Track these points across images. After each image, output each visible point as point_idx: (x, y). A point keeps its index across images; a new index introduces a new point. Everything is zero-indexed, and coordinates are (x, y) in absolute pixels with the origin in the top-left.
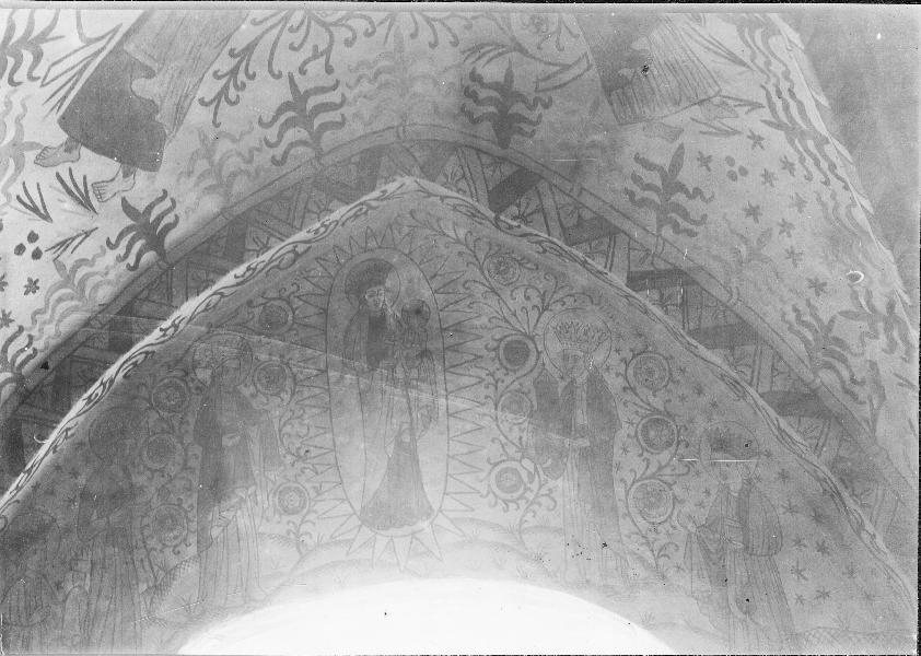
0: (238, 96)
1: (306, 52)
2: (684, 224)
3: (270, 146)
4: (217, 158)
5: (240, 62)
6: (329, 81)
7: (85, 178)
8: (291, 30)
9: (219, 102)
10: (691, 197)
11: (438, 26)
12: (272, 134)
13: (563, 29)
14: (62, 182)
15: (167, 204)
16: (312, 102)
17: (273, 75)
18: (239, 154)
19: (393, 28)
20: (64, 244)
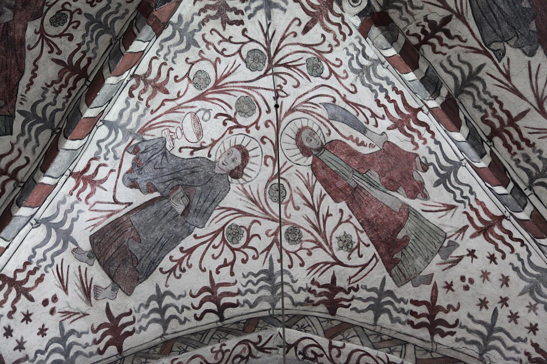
0: (180, 275)
1: (221, 261)
2: (446, 330)
3: (194, 308)
4: (163, 304)
5: (185, 256)
6: (231, 280)
7: (92, 278)
8: (214, 247)
9: (170, 274)
10: (446, 312)
11: (293, 256)
12: (196, 302)
13: (361, 243)
14: (80, 270)
15: (129, 319)
16: (220, 290)
17: (201, 268)
18: (176, 307)
19: (269, 256)
20: (67, 313)
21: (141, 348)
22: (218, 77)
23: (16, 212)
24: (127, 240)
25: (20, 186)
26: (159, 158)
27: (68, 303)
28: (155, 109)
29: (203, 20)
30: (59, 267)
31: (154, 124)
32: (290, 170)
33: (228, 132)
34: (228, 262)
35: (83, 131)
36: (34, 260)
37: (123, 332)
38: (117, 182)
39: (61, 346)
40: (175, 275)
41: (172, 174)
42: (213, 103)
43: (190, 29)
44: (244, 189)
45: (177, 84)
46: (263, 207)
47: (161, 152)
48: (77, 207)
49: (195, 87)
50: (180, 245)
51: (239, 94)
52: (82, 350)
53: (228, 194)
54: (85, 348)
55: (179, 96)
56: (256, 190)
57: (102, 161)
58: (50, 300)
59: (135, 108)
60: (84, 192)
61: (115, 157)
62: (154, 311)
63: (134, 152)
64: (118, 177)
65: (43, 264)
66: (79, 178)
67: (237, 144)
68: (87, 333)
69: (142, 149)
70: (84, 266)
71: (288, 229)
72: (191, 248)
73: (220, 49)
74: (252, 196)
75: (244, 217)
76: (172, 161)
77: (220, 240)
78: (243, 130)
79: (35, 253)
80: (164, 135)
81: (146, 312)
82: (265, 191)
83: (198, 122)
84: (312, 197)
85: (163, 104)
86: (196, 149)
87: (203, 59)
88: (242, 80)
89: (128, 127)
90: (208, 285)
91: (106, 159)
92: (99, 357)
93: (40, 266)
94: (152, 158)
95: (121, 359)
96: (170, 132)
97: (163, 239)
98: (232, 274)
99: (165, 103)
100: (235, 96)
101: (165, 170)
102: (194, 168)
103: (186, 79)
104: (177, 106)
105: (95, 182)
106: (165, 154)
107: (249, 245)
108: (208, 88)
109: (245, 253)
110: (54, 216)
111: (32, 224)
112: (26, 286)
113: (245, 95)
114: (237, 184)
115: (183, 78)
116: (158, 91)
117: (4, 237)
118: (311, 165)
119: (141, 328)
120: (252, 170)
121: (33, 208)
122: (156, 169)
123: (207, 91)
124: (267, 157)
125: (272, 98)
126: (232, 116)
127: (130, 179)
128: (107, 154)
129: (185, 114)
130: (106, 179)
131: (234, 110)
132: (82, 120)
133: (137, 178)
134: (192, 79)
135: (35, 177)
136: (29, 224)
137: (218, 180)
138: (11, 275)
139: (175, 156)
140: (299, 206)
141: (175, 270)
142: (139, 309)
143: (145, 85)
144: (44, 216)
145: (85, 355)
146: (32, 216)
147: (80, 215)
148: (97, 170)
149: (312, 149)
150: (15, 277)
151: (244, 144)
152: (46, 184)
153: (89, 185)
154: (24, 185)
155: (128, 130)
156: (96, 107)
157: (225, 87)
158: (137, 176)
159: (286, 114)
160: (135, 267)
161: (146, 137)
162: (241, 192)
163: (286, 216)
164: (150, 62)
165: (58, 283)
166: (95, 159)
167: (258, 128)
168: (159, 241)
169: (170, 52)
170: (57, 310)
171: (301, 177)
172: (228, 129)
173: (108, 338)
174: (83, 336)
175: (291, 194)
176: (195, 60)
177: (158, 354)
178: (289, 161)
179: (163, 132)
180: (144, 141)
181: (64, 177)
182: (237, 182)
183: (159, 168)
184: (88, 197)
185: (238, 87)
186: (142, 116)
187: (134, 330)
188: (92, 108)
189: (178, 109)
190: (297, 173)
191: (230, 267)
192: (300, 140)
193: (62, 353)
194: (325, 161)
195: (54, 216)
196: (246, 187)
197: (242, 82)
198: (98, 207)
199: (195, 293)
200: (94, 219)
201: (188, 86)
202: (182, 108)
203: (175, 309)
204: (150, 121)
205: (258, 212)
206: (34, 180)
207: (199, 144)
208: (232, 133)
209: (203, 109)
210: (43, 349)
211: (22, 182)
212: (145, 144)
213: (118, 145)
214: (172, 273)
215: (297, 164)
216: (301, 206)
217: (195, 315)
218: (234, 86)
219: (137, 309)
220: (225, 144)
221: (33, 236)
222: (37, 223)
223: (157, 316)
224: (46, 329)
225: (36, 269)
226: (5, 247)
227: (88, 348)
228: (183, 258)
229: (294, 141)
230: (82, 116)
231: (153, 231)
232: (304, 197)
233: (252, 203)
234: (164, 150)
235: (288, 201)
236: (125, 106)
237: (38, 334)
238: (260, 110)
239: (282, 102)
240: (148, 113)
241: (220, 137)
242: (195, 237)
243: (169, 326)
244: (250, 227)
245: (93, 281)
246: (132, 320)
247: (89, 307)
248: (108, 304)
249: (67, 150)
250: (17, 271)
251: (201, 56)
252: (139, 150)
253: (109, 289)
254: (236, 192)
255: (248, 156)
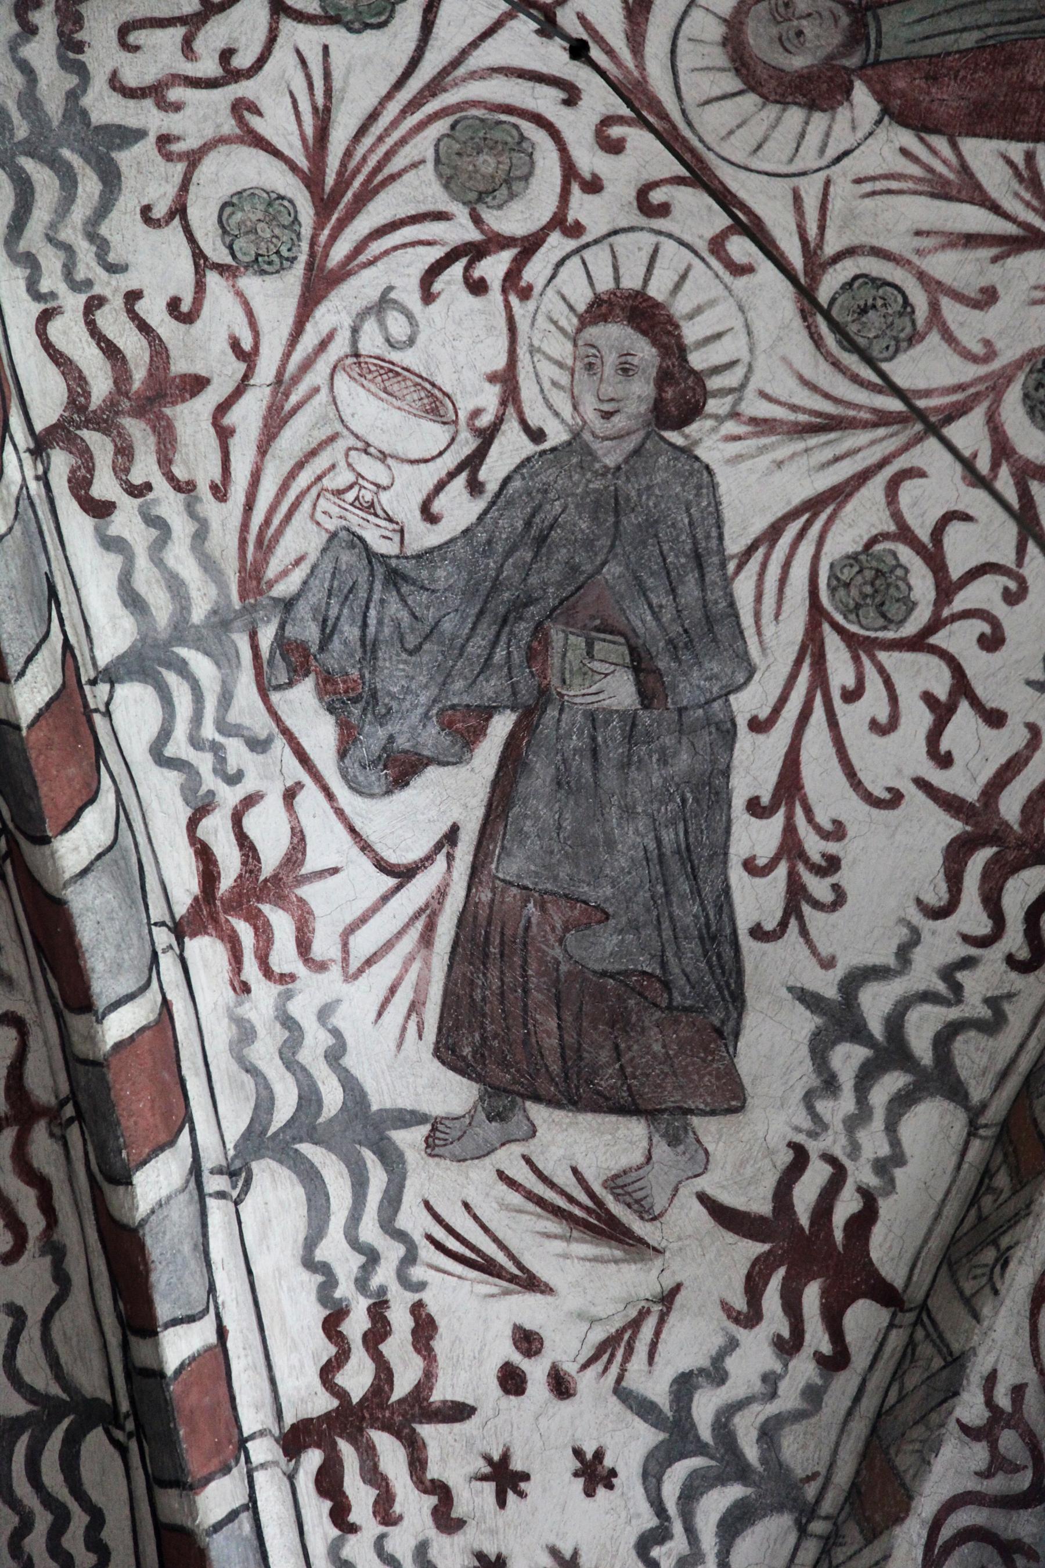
0: (836, 888)
4: (876, 1028)
5: (790, 818)
7: (575, 1171)
8: (851, 696)
9: (800, 918)
14: (512, 1183)
15: (816, 1175)
17: (877, 803)
18: (927, 997)
21: (945, 1227)
22: (303, 163)
23: (134, 1207)
24: (558, 952)
25: (71, 1121)
26: (394, 607)
27: (581, 1316)
28: (216, 475)
29: (60, 34)
30: (440, 1234)
31: (267, 522)
32: (836, 205)
33: (514, 300)
34: (942, 693)
35: (72, 771)
36: (345, 1289)
37: (839, 1235)
38: (340, 813)
39: (697, 1462)
40: (817, 905)
41: (481, 613)
42: (371, 263)
43: (54, 107)
44: (753, 421)
45: (199, 324)
46: (874, 411)
47: (378, 586)
48: (303, 1009)
49: (263, 272)
50: (739, 802)
51: (423, 145)
52: (772, 1409)
53: (722, 490)
54: (773, 1395)
55: (248, 357)
56: (792, 383)
57: (229, 797)
58: (517, 1358)
59: (154, 533)
60: (277, 945)
61: (258, 745)
62: (866, 1077)
63: (298, 670)
64: (330, 796)
65: (384, 1275)
66: (215, 920)
67: (581, 308)
68: (732, 1345)
69: (311, 633)
70: (509, 1158)
71: (1026, 396)
72: (782, 777)
73: (208, 67)
74: (802, 418)
75: (849, 507)
76: (441, 573)
77: (845, 655)
78: (557, 244)
79: (324, 1269)
80: (331, 525)
81: (847, 1103)
82: (828, 356)
83: (393, 371)
84: (996, 209)
85: (224, 434)
86: (473, 462)
87: (194, 159)
88: (383, 92)
89: (198, 614)
90: (952, 827)
91: (234, 779)
92: (845, 1383)
93: (382, 1290)
94: (372, 630)
95: (918, 1321)
96: (339, 493)
97: (668, 836)
98: (995, 718)
99: (228, 420)
100: (414, 165)
101: (447, 626)
102: (528, 524)
103: (212, 279)
104: (274, 394)
105: (276, 878)
106: (395, 577)
107: (956, 572)
108: (306, 231)
109: (967, 614)
110: (265, 1104)
111: (221, 1195)
112: (402, 1386)
113: (441, 126)
114: (714, 430)
115: (200, 287)
116: (168, 411)
117: (179, 1313)
118: (885, 111)
119: (883, 1167)
120: (719, 336)
121: (172, 1143)
122: (418, 648)
123: (313, 243)
124: (717, 246)
125: (536, 39)
126: (473, 235)
127: (374, 763)
128: (221, 760)
129: (324, 391)
130: (299, 839)
131: (461, 213)
132: (34, 740)
133: (391, 739)
134: (228, 260)
135: (81, 1048)
136: (212, 1203)
137: (644, 482)
138: (323, 1403)
139: (431, 551)
140: (984, 282)
141: (803, 888)
142: (816, 1117)
143: (106, 432)
144: (234, 1131)
145: (798, 1416)
146: (196, 1169)
147: (337, 1020)
148: (243, 840)
149: (831, 57)
150: (341, 1394)
151: (605, 283)
152: (132, 1038)
153: (266, 909)
154: (77, 1106)
155: (207, 624)
156: (30, 659)
157: (357, 170)
158: (382, 733)
159: (636, 40)
160: (670, 1007)
161: (282, 590)
162: (752, 443)
163: (975, 359)
164: (48, 346)
165: (489, 1285)
166: (200, 811)
167: (594, 186)
168: (661, 856)
169: (68, 249)
170: (570, 1368)
171: (894, 185)
172: (504, 291)
173: (812, 1296)
174: (731, 1363)
175: (922, 277)
176: (171, 190)
177: (1015, 1192)
178: (802, 183)
179: (319, 516)
180: (288, 605)
181: (168, 964)
182: (709, 423)
183: (427, 637)
184: (303, 946)
185: (395, 124)
186: (201, 535)
187: (868, 1197)
188: (22, 674)
189: (287, 395)
190: (868, 187)
191: (964, 707)
192: (762, 73)
193: (721, 1480)
194: (914, 49)
195: (265, 1104)
196: (755, 407)
197: (389, 96)
198: (364, 943)
199: (937, 894)
200: (393, 990)
201: (239, 294)
202: (296, 380)
203: (927, 1008)
204: (245, 526)
205: (873, 443)
206: (85, 1062)
207: (465, 435)
208: (530, 288)
209: (362, 316)
210: (648, 1521)
211: (62, 1104)
212: (303, 609)
213: (226, 698)
214: (806, 909)
215: (838, 159)
216: (994, 275)
217: (1011, 960)
218: (380, 139)
219: (806, 1123)
220: (545, 347)
221: (265, 1224)
222: (233, 1174)
223: (893, 1082)
224: (599, 1455)
225: (378, 1311)
226: (212, 1338)
227: (783, 1386)
228: (790, 829)
229: (751, 100)
230: (18, 728)
231: (610, 844)
232: (971, 240)
233: (823, 438)
234: (380, 571)
235: (935, 308)
236: (116, 561)
237: (589, 1492)
238: (539, 120)
239: (581, 18)
240: (209, 506)
241: (504, 343)
242: (758, 726)
243: (963, 1074)
244: (897, 516)
245: (589, 1175)
246: (827, 1170)
247: (658, 1263)
248: (703, 1198)
249: (84, 872)
250: (327, 1373)
251: (180, 156)
252: (302, 647)
253: (662, 1150)
254: (739, 458)
255: (657, 305)
